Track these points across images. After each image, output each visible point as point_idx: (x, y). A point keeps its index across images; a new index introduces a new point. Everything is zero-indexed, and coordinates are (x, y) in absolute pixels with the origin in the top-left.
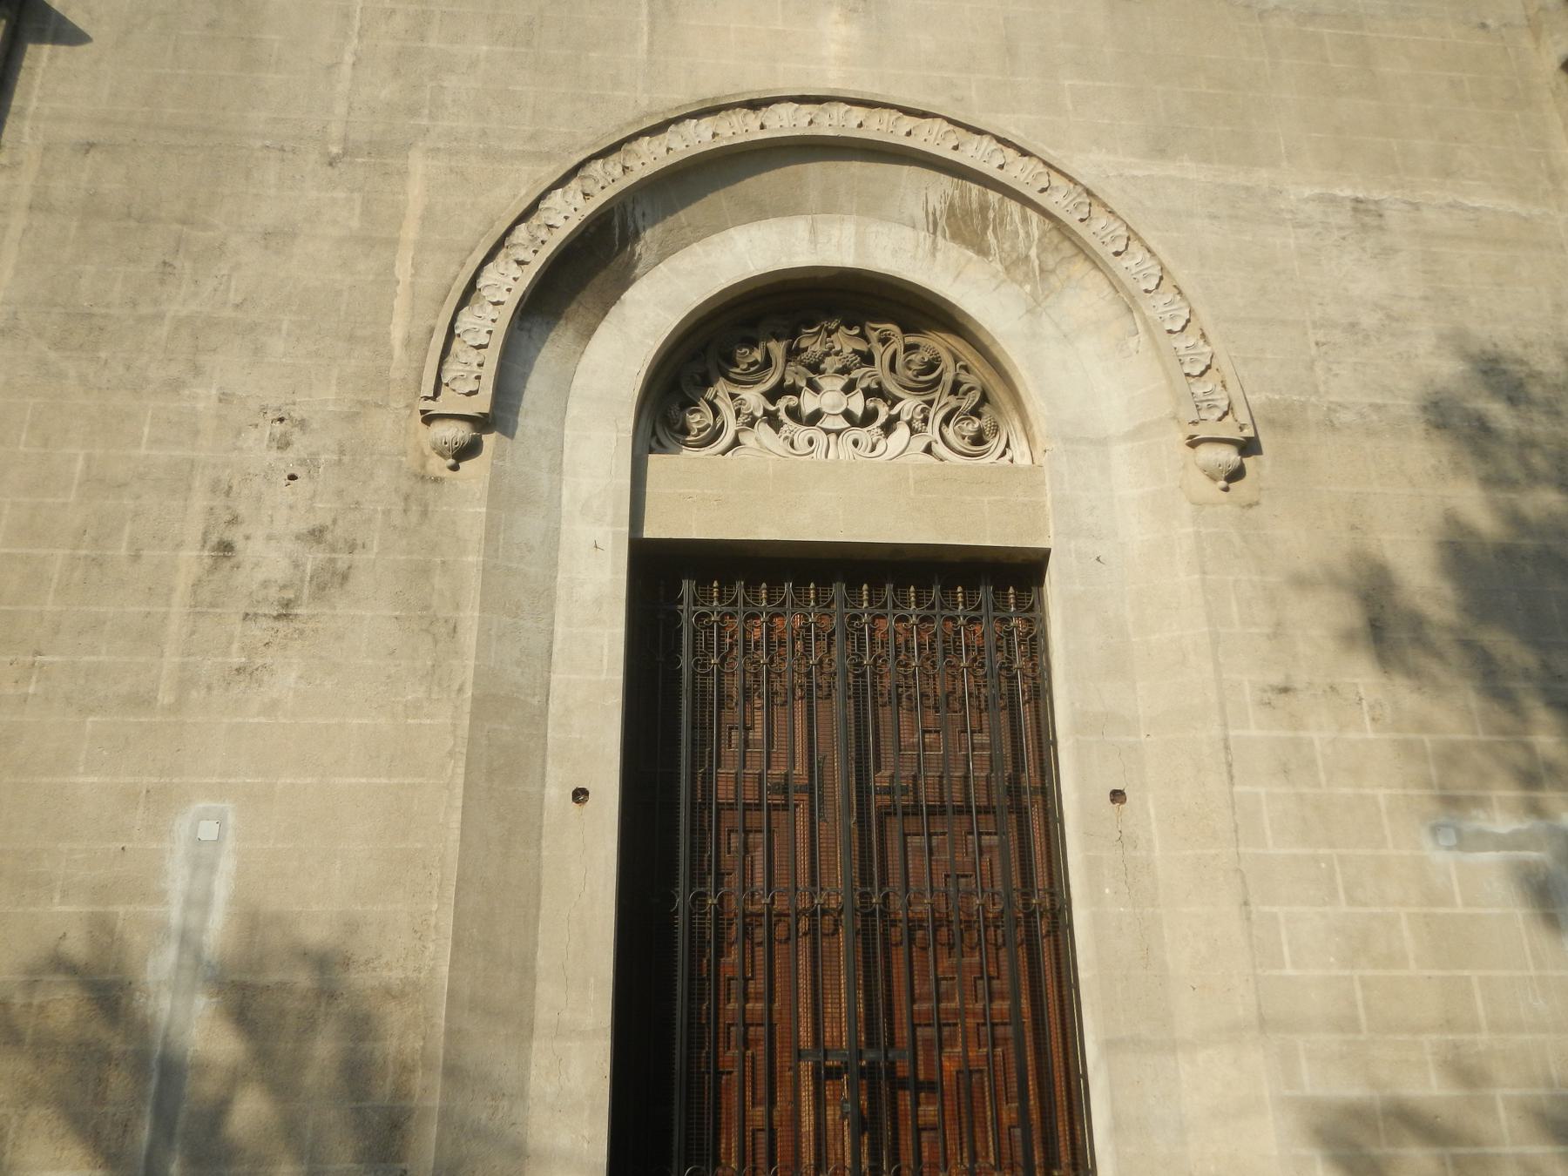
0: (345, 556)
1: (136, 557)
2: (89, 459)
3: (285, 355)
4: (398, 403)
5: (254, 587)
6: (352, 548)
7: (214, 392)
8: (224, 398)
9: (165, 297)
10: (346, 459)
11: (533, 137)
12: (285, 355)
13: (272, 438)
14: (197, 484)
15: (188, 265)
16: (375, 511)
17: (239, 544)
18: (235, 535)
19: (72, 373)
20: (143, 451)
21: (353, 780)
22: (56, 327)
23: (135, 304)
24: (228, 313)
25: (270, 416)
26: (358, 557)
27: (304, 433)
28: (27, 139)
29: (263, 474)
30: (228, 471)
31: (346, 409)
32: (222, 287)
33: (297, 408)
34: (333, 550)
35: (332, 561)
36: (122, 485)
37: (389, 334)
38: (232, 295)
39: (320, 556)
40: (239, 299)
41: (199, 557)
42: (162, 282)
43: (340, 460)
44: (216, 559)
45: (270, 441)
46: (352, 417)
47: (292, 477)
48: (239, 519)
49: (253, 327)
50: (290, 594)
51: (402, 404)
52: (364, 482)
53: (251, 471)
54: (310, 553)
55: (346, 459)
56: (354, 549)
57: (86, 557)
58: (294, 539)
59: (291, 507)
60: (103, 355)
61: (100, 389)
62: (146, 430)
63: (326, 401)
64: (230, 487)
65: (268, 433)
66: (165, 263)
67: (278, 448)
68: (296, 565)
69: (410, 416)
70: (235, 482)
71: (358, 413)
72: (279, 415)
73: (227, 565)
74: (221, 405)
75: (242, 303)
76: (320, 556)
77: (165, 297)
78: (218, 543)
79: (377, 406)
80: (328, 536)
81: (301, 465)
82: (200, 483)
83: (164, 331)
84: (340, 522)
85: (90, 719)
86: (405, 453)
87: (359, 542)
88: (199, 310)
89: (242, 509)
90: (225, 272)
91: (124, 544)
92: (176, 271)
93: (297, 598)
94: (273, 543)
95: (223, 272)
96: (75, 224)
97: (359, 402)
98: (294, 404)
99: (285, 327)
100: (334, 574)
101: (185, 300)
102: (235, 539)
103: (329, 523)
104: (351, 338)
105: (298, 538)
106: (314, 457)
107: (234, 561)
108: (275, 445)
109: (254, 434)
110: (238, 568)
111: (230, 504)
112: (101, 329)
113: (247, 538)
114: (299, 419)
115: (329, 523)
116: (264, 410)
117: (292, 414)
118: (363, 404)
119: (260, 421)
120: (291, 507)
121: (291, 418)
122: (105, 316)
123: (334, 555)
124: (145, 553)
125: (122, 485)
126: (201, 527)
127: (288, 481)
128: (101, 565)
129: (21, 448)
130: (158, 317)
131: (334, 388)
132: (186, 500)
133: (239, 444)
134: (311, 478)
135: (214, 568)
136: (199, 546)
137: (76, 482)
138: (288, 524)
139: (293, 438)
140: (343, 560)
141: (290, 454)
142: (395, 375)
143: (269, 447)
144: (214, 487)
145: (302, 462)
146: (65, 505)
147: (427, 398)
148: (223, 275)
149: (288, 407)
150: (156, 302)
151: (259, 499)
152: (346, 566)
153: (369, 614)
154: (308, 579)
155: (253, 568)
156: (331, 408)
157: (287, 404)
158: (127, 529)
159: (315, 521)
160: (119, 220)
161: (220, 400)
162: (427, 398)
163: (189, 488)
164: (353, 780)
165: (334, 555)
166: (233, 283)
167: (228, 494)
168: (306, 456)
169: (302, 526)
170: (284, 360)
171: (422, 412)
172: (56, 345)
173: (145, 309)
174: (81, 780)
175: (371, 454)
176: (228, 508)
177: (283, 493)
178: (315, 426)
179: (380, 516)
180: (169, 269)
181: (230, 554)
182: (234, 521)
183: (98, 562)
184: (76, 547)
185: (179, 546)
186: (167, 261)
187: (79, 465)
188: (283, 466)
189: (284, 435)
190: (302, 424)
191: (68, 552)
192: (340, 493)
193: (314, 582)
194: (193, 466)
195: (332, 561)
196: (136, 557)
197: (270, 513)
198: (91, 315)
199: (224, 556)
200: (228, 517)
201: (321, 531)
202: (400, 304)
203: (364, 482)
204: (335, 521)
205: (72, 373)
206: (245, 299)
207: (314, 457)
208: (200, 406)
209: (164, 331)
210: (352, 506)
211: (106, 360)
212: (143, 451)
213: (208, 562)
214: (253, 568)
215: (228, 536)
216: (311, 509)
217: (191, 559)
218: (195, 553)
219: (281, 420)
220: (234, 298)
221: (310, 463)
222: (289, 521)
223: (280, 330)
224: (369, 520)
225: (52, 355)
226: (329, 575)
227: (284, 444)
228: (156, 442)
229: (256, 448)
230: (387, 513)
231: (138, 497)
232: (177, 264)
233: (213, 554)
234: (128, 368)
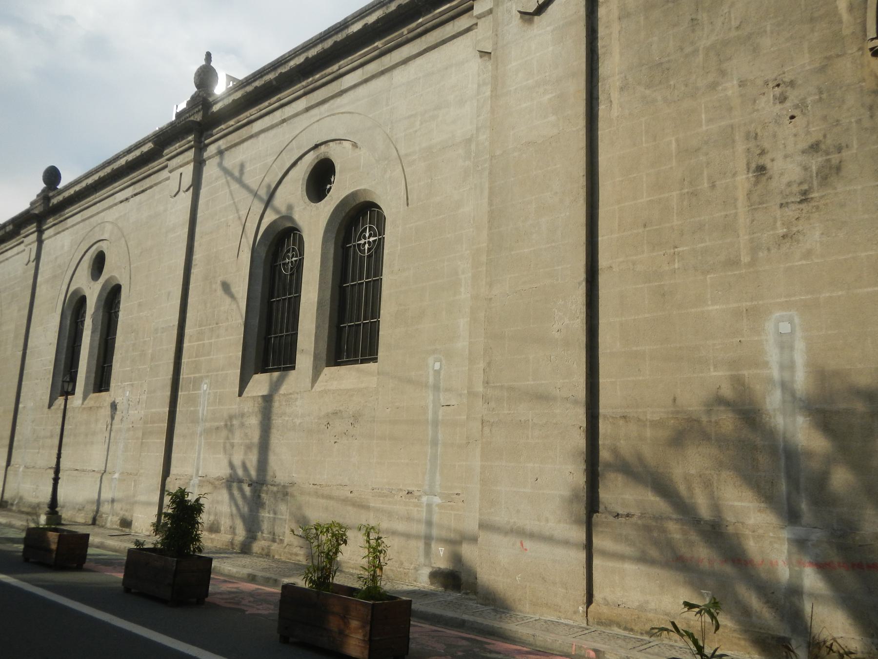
0: (837, 156)
1: (713, 186)
2: (677, 140)
3: (772, 46)
4: (852, 50)
5: (783, 188)
6: (839, 149)
7: (735, 82)
8: (742, 84)
9: (697, 38)
10: (824, 96)
12: (772, 46)
13: (775, 97)
14: (737, 137)
15: (705, 15)
16: (850, 122)
17: (769, 165)
18: (766, 161)
19: (659, 98)
20: (704, 128)
21: (870, 289)
22: (646, 77)
23: (682, 49)
24: (734, 33)
25: (771, 85)
26: (845, 154)
27: (794, 89)
29: (774, 120)
30: (753, 125)
31: (817, 65)
32: (727, 20)
33: (786, 75)
34: (827, 153)
35: (829, 161)
36: (698, 150)
37: (837, 7)
38: (733, 23)
39: (820, 159)
40: (738, 23)
41: (747, 178)
42: (693, 31)
43: (821, 98)
44: (757, 177)
45: (774, 100)
46: (823, 69)
47: (792, 117)
48: (766, 151)
49: (749, 37)
50: (805, 187)
51: (855, 49)
52: (839, 107)
53: (766, 121)
54: (813, 159)
55: (824, 96)
56: (842, 149)
57: (688, 193)
58: (800, 153)
59: (795, 135)
60: (672, 83)
61: (675, 102)
62: (703, 116)
63: (805, 64)
64: (756, 134)
65: (772, 96)
66: (692, 19)
67: (780, 103)
68: (806, 169)
69: (863, 54)
70: (758, 131)
71: (827, 65)
72: (776, 83)
73: (764, 178)
74: (741, 88)
75: (740, 26)
76: (820, 159)
77: (697, 38)
78: (756, 167)
79: (838, 56)
80: (823, 147)
81: (796, 108)
82: (739, 136)
83: (701, 57)
84: (828, 136)
85: (708, 276)
86: (864, 80)
87: (844, 145)
88: (716, 38)
89: (766, 145)
90: (726, 10)
91: (706, 181)
92: (699, 22)
93: (810, 188)
94: (789, 160)
95: (725, 11)
96: (642, 18)
97: (826, 58)
98: (784, 73)
99: (768, 28)
100: (831, 168)
101: (708, 36)
102: (766, 163)
103: (821, 138)
104: (812, 20)
105: (803, 152)
106: (803, 101)
107: (767, 175)
108: (777, 101)
109: (764, 99)
110: (771, 179)
111: (758, 144)
112: (668, 69)
113: (773, 160)
114: (789, 81)
115: (821, 138)
116: (766, 83)
117: (784, 80)
118: (828, 58)
119: (766, 90)
120: (795, 135)
121: (784, 82)
122: (669, 61)
123: (829, 157)
124: (717, 183)
125: (698, 150)
126: (745, 161)
127: (790, 120)
128: (696, 195)
129: (644, 145)
130: (696, 51)
131: (807, 55)
132: (733, 149)
133: (756, 108)
134: (804, 114)
135: (757, 183)
136: (745, 172)
137: (674, 154)
138: (795, 146)
139: (788, 94)
140: (835, 158)
141: (788, 104)
142: (846, 32)
143: (774, 104)
144: (747, 136)
145: (796, 107)
146: (671, 168)
147: (872, 39)
148: (725, 14)
149: (780, 77)
150: (692, 43)
151: (775, 136)
152: (838, 162)
153: (859, 187)
154: (814, 175)
155: (780, 177)
156: (808, 68)
157: (779, 75)
158: (705, 173)
159: (811, 140)
160: (663, 6)
161: (740, 86)
162: (872, 39)
163: (734, 141)
164: (870, 289)
165: (829, 157)
166: (732, 15)
167: (756, 138)
168: (798, 103)
169: (803, 145)
170: (772, 49)
171: (871, 49)
172: (648, 86)
173: (688, 49)
174: (710, 308)
175: (841, 88)
176: (758, 146)
177: (788, 128)
178: (800, 82)
179: (854, 125)
180: (695, 22)
181: (764, 172)
182: (763, 152)
183: (694, 194)
184: (682, 189)
185: (735, 175)
186: (693, 18)
187: (674, 146)
188: (785, 113)
189: (782, 93)
190: (792, 84)
191: (678, 192)
192: (825, 118)
193: (819, 177)
194: (732, 128)
195: (829, 161)
196: (713, 186)
197: (783, 142)
198: (662, 63)
199: (761, 174)
200: (759, 152)
201: (817, 145)
203: (839, 107)
204: (825, 136)
205: (659, 98)
206: (741, 22)
207: (803, 101)
208: (730, 93)
209: (701, 57)
210: (834, 124)
211: (674, 85)
212: (704, 128)
213: (753, 180)
214: (780, 177)
215: (761, 162)
216: (808, 133)
217: (743, 180)
218: (744, 177)
219: (778, 85)
220: (734, 23)
221: (802, 106)
222: (795, 144)
223: (765, 31)
224: (848, 129)
225: (648, 92)
226: (828, 169)
227: (783, 99)
228: (710, 121)
229: (767, 107)
230: (859, 121)
231: (707, 154)
232: (699, 17)
233: (755, 174)
234: (686, 85)
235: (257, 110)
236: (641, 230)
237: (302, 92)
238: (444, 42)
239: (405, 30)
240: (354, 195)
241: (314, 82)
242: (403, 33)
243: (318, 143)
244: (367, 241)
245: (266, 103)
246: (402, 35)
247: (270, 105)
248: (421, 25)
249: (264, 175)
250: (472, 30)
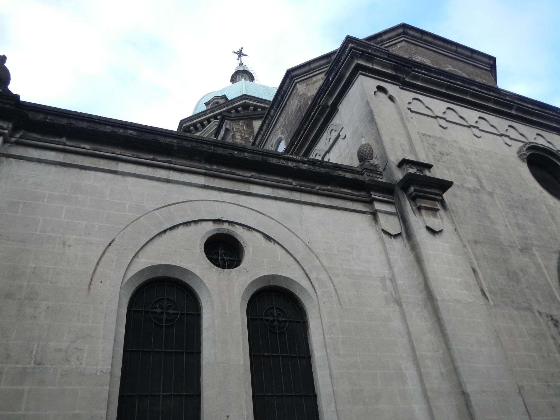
11: (551, 248)
28: (463, 239)
202: (554, 289)
235: (133, 155)
236: (529, 369)
237: (203, 171)
238: (346, 210)
239: (318, 187)
240: (274, 277)
241: (219, 171)
242: (315, 187)
243: (222, 219)
244: (276, 319)
245: (151, 157)
246: (314, 188)
247: (154, 160)
248: (341, 192)
249: (139, 216)
250: (366, 214)
